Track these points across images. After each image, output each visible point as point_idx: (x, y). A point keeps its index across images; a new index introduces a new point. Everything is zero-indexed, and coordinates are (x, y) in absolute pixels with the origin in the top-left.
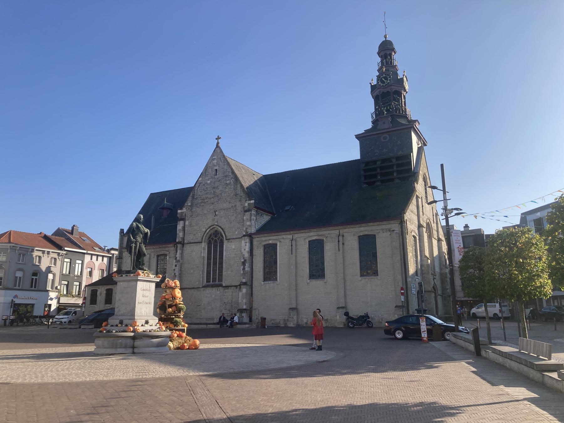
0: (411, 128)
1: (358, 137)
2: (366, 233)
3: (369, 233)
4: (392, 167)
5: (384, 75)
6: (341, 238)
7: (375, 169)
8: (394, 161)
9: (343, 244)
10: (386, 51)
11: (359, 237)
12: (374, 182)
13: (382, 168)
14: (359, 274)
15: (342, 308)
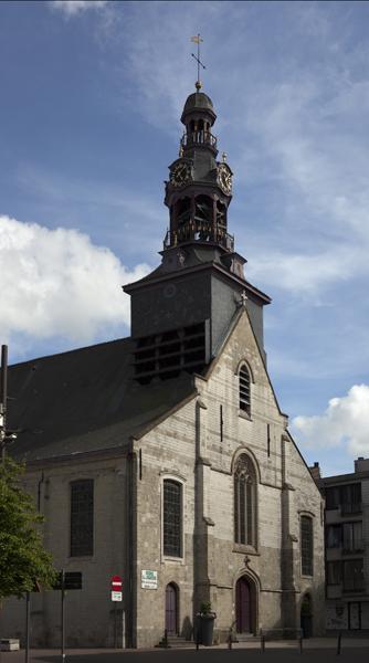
0: (209, 270)
1: (127, 289)
2: (81, 476)
3: (86, 477)
4: (176, 347)
5: (181, 166)
6: (43, 485)
7: (176, 347)
8: (182, 337)
9: (47, 497)
10: (198, 115)
11: (71, 483)
12: (151, 378)
13: (163, 350)
14: (67, 551)
15: (38, 613)
